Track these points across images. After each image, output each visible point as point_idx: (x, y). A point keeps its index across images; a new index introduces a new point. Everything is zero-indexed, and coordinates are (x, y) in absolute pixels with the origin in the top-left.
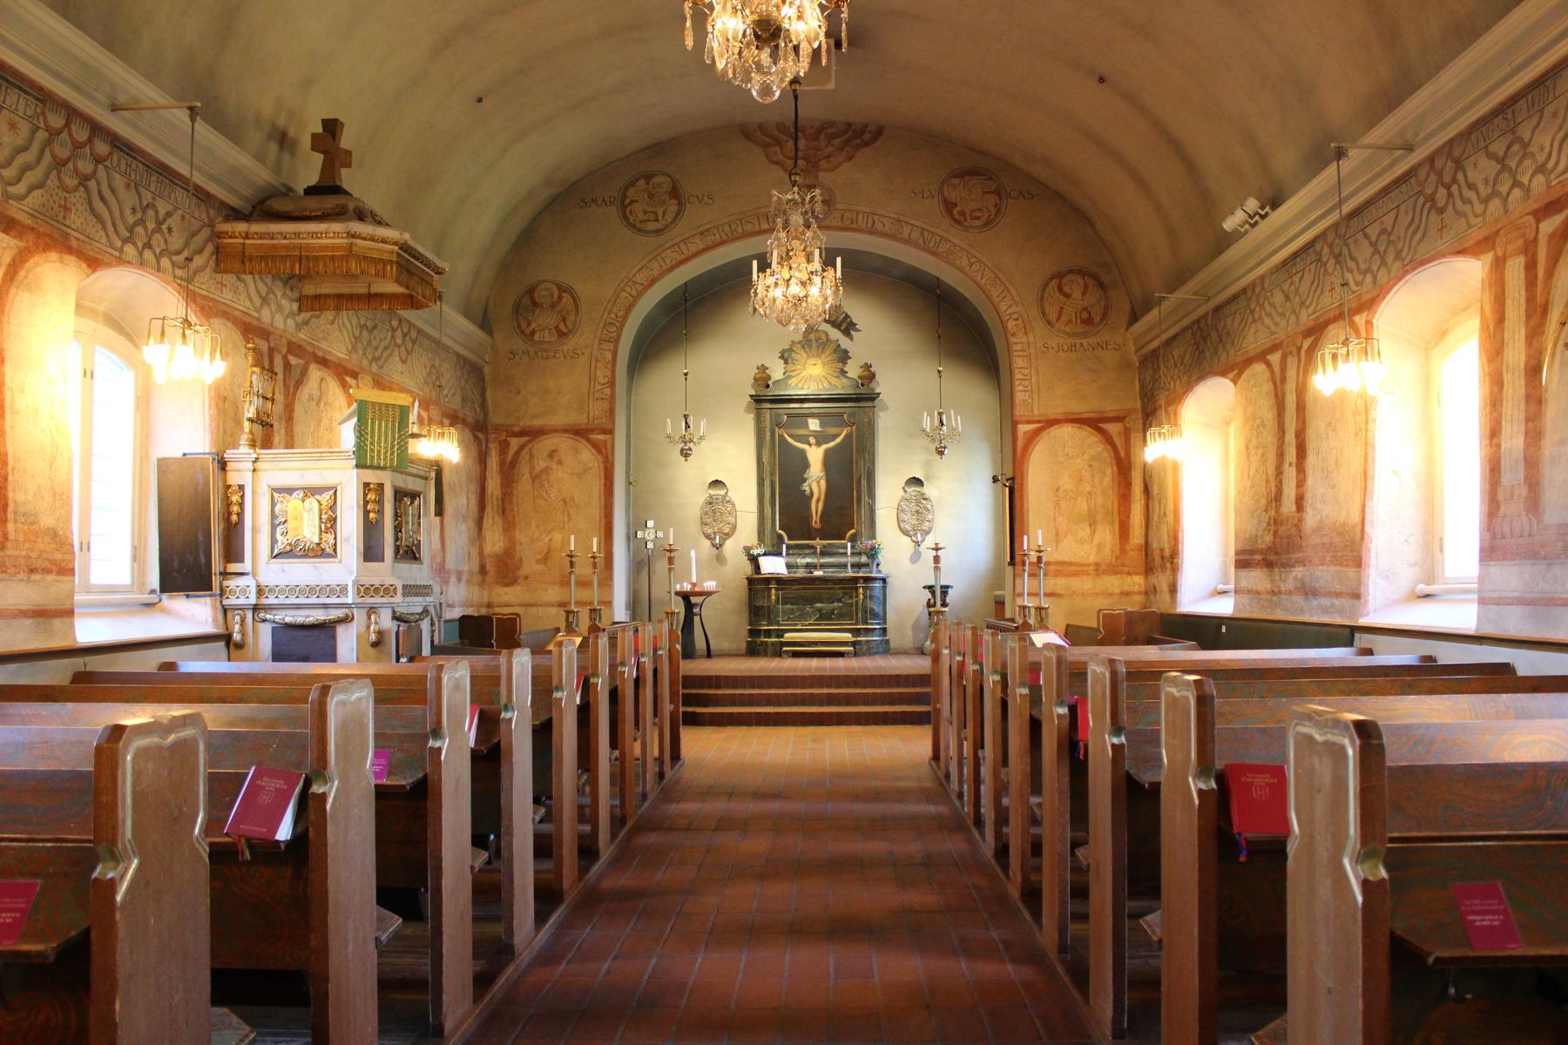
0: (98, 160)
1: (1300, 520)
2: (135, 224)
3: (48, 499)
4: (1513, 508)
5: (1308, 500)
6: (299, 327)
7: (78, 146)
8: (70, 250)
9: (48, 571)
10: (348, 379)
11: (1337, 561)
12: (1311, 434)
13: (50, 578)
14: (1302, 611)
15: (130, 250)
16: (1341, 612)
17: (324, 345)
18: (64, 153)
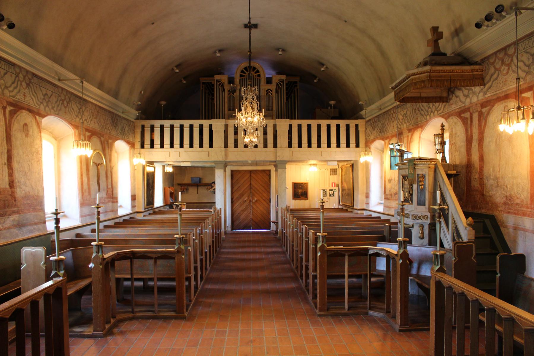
1: (13, 193)
4: (86, 194)
5: (16, 184)
6: (485, 93)
11: (35, 210)
12: (15, 152)
14: (17, 235)
15: (428, 117)
16: (39, 230)
17: (505, 89)
18: (415, 108)
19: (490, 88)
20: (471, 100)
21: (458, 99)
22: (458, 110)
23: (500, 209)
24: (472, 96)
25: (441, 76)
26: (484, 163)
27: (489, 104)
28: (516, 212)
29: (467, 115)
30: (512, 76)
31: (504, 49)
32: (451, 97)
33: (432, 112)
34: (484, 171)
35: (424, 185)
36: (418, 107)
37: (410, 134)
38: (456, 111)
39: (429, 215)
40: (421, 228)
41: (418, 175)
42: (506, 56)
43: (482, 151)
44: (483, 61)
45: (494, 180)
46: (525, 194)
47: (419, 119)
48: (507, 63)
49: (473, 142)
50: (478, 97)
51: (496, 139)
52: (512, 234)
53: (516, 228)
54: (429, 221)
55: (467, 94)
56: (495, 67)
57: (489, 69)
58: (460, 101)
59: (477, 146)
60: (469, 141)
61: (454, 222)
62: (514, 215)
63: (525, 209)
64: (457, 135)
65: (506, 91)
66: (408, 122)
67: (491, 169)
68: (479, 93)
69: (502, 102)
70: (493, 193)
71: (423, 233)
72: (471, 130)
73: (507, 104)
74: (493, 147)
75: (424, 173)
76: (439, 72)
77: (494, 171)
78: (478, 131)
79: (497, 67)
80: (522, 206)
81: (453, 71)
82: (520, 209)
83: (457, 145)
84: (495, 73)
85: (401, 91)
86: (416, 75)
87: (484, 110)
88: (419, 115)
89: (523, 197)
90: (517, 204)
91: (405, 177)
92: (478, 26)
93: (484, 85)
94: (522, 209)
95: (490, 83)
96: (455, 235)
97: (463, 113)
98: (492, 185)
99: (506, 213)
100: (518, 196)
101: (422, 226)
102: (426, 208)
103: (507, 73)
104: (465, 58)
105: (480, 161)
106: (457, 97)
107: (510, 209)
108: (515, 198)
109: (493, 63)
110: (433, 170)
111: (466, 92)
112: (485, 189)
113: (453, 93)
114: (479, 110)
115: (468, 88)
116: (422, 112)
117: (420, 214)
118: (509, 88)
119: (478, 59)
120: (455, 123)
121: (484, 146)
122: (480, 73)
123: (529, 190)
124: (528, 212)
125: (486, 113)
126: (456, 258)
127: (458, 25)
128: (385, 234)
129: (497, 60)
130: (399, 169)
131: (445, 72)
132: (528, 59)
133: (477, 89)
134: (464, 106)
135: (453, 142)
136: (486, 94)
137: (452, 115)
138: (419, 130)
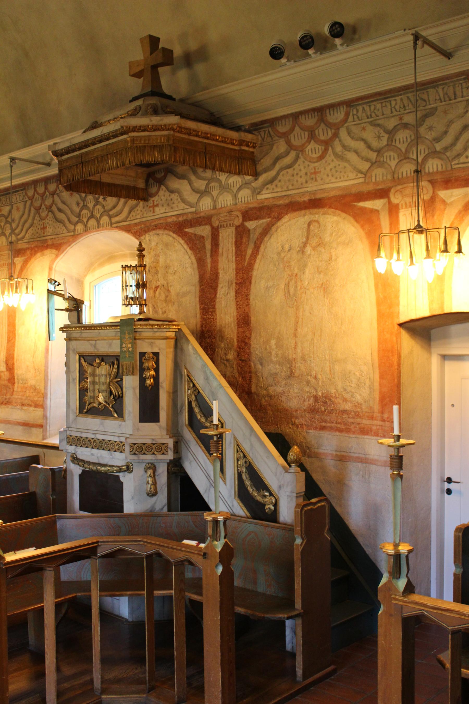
0: (53, 194)
2: (81, 211)
3: (32, 371)
6: (256, 192)
7: (43, 195)
8: (47, 247)
9: (31, 406)
10: (368, 204)
13: (32, 408)
15: (80, 227)
17: (312, 187)
18: (37, 204)
19: (271, 181)
20: (215, 201)
21: (175, 196)
22: (175, 219)
23: (297, 421)
24: (219, 194)
25: (191, 143)
26: (250, 330)
27: (272, 213)
28: (343, 427)
29: (204, 231)
30: (332, 166)
31: (320, 111)
32: (153, 190)
33: (92, 216)
34: (253, 345)
35: (156, 378)
36: (48, 202)
37: (19, 261)
38: (170, 220)
39: (170, 442)
40: (150, 472)
41: (142, 355)
42: (322, 125)
43: (248, 305)
44: (255, 128)
45: (280, 364)
46: (365, 392)
47: (49, 230)
48: (322, 138)
49: (220, 286)
50: (235, 196)
51: (287, 285)
52: (333, 470)
53: (342, 458)
54: (170, 456)
55: (203, 188)
56: (288, 143)
57: (272, 146)
58: (183, 201)
59: (233, 294)
60: (208, 286)
61: (241, 454)
62: (338, 433)
63: (364, 422)
64: (171, 271)
65: (314, 193)
66: (13, 231)
67: (273, 342)
68: (239, 189)
69: (303, 212)
70: (279, 389)
71: (155, 483)
72: (215, 262)
73: (316, 217)
74: (278, 298)
75: (156, 350)
76: (189, 134)
77: (279, 345)
78: (233, 265)
79: (296, 142)
80: (357, 415)
81: (212, 137)
82: (352, 420)
83: (171, 289)
84: (287, 154)
85: (82, 162)
86: (144, 131)
87: (251, 225)
88: (50, 221)
89: (358, 398)
90: (344, 412)
91: (87, 359)
92: (276, 53)
93: (256, 175)
94: (358, 420)
95: (272, 173)
96: (248, 483)
97: (191, 226)
98: (276, 374)
99: (316, 428)
100: (347, 396)
101: (152, 467)
102: (160, 427)
103: (321, 158)
104: (212, 114)
105: (239, 326)
106: (172, 192)
107: (326, 421)
108: (340, 400)
109: (285, 135)
110: (172, 342)
111: (201, 184)
112: (254, 380)
113: (161, 182)
114: (238, 222)
115: (209, 173)
116: (61, 216)
117: (148, 441)
118: (323, 187)
119: (245, 122)
120: (166, 245)
121: (252, 297)
122: (251, 150)
123: (377, 386)
124: (374, 428)
125: (259, 231)
126: (303, 539)
127: (193, 46)
128: (32, 489)
129: (297, 128)
130: (69, 339)
131: (197, 136)
132: (379, 137)
133: (235, 180)
134: (196, 213)
135: (159, 284)
136: (259, 193)
137: (156, 227)
138: (49, 255)
